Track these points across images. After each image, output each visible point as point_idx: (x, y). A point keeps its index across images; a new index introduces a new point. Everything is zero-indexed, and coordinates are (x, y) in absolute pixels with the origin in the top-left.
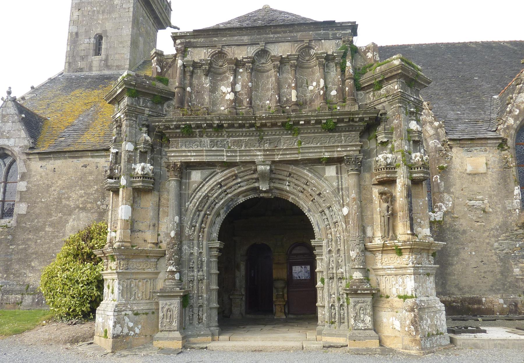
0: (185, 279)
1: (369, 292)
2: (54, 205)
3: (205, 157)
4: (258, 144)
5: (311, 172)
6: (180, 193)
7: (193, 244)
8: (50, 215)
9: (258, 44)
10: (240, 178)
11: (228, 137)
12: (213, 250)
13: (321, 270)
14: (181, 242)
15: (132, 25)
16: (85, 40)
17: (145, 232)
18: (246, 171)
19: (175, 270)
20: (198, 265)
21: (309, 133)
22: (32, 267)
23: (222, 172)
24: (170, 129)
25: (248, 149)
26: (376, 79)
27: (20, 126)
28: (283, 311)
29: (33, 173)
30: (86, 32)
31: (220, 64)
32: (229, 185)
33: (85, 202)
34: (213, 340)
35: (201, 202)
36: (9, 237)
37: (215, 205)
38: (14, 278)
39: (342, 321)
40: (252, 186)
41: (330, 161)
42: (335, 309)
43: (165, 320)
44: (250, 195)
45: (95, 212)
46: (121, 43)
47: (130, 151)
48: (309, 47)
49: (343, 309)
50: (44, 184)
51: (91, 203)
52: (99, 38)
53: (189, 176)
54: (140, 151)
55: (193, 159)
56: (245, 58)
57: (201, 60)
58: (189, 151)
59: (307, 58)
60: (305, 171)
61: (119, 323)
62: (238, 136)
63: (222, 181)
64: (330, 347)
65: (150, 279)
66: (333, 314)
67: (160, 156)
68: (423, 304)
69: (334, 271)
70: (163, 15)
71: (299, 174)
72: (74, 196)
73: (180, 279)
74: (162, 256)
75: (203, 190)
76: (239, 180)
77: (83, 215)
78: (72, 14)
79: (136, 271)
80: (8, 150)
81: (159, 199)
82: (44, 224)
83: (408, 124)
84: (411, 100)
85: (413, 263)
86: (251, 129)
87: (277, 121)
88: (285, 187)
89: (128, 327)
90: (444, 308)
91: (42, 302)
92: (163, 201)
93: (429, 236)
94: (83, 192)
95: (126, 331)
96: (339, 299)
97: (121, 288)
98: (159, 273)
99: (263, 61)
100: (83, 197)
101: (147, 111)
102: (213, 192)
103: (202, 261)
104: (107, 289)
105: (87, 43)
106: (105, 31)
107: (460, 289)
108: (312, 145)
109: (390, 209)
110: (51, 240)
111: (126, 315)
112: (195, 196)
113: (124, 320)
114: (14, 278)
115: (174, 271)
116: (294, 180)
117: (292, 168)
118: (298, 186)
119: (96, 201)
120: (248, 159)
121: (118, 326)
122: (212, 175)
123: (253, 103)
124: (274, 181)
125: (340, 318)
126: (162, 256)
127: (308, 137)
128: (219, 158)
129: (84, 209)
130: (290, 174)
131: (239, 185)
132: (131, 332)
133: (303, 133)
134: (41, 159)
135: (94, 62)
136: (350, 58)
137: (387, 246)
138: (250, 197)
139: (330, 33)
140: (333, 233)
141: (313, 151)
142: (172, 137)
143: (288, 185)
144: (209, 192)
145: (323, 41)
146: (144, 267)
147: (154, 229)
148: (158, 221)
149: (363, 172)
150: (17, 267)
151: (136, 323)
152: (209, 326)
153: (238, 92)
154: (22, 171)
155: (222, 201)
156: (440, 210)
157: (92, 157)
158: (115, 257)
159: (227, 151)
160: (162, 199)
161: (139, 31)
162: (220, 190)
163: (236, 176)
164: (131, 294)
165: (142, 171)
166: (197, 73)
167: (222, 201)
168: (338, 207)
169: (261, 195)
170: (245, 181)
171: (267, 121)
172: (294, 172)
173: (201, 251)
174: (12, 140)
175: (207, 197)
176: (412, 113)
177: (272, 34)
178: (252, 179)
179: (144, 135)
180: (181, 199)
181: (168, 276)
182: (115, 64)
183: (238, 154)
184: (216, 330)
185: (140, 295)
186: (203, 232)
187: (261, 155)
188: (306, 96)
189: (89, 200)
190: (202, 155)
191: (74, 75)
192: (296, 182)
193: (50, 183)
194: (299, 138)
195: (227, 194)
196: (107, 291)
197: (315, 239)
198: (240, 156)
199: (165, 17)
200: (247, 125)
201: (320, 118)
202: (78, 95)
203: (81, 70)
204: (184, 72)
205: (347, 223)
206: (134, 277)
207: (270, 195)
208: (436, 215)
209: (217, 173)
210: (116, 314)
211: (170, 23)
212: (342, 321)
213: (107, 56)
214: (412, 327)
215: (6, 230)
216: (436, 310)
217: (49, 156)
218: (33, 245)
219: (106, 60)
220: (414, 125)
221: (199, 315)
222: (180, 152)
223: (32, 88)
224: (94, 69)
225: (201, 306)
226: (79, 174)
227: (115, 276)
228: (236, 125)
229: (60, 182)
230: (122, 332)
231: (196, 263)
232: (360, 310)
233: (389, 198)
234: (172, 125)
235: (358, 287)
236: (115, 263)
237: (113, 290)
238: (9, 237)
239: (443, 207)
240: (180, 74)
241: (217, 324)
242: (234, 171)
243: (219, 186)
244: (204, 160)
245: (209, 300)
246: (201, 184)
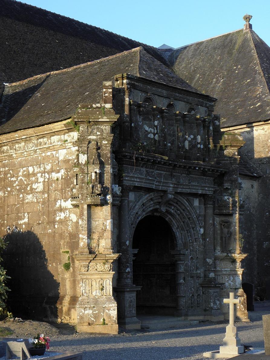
3: (143, 184)
116: (177, 206)
143: (173, 209)
145: (199, 106)
172: (180, 200)
177: (178, 93)
183: (161, 184)
190: (142, 182)
192: (179, 208)
196: (110, 288)
198: (162, 186)
205: (204, 239)
214: (242, 306)
244: (143, 186)
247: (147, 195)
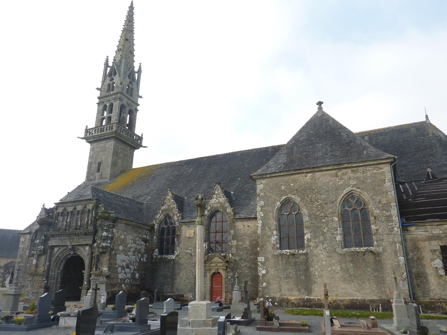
30: (95, 161)
46: (107, 166)
52: (100, 164)
95: (29, 298)
105: (95, 166)
106: (102, 161)
107: (178, 290)
117: (79, 247)
120: (66, 244)
122: (60, 249)
151: (33, 296)
163: (65, 250)
175: (58, 256)
213: (102, 173)
219: (101, 175)
223: (68, 193)
246: (57, 252)
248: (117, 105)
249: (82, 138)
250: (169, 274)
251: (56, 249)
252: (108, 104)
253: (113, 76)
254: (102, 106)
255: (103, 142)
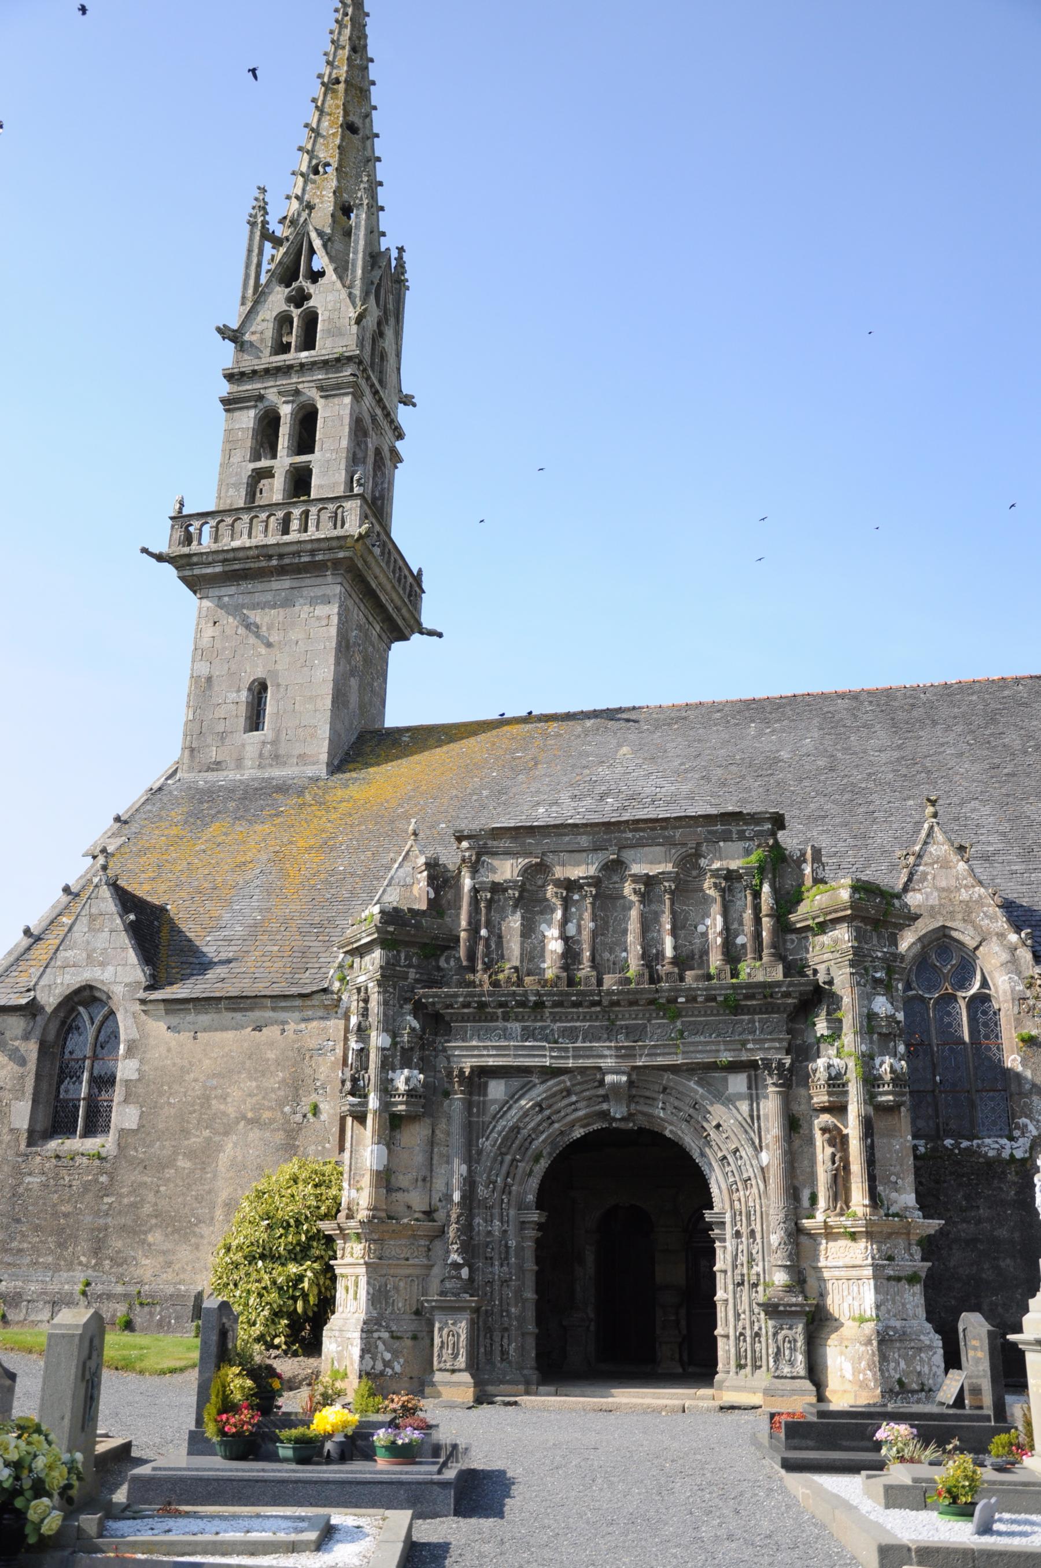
0: (479, 1278)
1: (798, 1309)
2: (195, 1111)
4: (605, 1036)
5: (702, 1087)
6: (470, 1122)
7: (491, 1216)
8: (185, 1132)
9: (607, 849)
10: (576, 1094)
11: (554, 1021)
12: (527, 1226)
13: (724, 1268)
14: (471, 1210)
15: (336, 656)
16: (228, 694)
17: (408, 1191)
18: (586, 1082)
19: (461, 1262)
20: (500, 1253)
21: (697, 1016)
22: (150, 1245)
23: (542, 1083)
24: (453, 1008)
25: (588, 1044)
26: (814, 919)
27: (124, 940)
28: (677, 1356)
29: (152, 1042)
30: (231, 674)
31: (540, 883)
32: (556, 1107)
33: (257, 1108)
34: (527, 1393)
35: (505, 1139)
36: (103, 1179)
37: (530, 1143)
38: (111, 1268)
39: (758, 1364)
40: (597, 1108)
41: (734, 1067)
42: (745, 1341)
43: (444, 1351)
44: (593, 1124)
45: (278, 1130)
47: (383, 1049)
48: (698, 855)
49: (760, 1342)
50: (174, 1065)
51: (270, 1108)
52: (259, 690)
53: (483, 1089)
54: (402, 1047)
55: (491, 1062)
56: (583, 878)
57: (505, 881)
58: (486, 1048)
59: (694, 873)
60: (692, 1084)
61: (369, 1351)
62: (572, 1020)
63: (542, 1099)
64: (733, 1408)
65: (417, 1277)
66: (742, 1350)
67: (434, 1053)
68: (891, 1333)
69: (745, 1271)
70: (404, 611)
71: (681, 1089)
72: (235, 1093)
73: (471, 1279)
74: (437, 1236)
75: (508, 1116)
76: (574, 1098)
77: (254, 1134)
78: (199, 631)
79: (395, 1262)
80: (100, 990)
81: (433, 1131)
82: (175, 1153)
83: (870, 1002)
84: (877, 957)
85: (873, 1258)
86: (593, 1009)
87: (638, 997)
88: (656, 1112)
89: (384, 1360)
90: (940, 1344)
91: (170, 1322)
92: (440, 1135)
93: (913, 1208)
94: (254, 1084)
95: (379, 1366)
96: (752, 1323)
97: (371, 1291)
98: (432, 1266)
99: (616, 878)
100: (255, 1095)
101: (412, 974)
102: (527, 1119)
103: (507, 1247)
104: (344, 1292)
106: (274, 673)
108: (702, 1039)
109: (837, 1158)
110: (189, 1187)
111: (379, 1338)
112: (495, 1127)
113: (377, 1347)
114: (111, 1268)
115: (459, 1264)
116: (672, 1099)
117: (668, 1078)
118: (680, 1110)
119: (281, 1104)
121: (367, 1356)
123: (598, 957)
124: (636, 1100)
125: (754, 1359)
126: (437, 1236)
127: (694, 1023)
128: (537, 1060)
129: (254, 1122)
130: (665, 1089)
131: (573, 1107)
132: (387, 1369)
133: (686, 1016)
134: (168, 1012)
135: (248, 748)
136: (770, 876)
137: (831, 1227)
138: (595, 1127)
139: (734, 829)
140: (743, 1200)
141: (704, 1048)
142: (456, 1021)
144: (520, 1120)
145: (721, 844)
146: (408, 1255)
147: (424, 1187)
148: (431, 1171)
149: (797, 1086)
150: (119, 1244)
151: (396, 1354)
152: (521, 1368)
153: (572, 937)
154: (131, 1037)
155: (544, 1136)
156: (1023, 1135)
157: (274, 1009)
158: (362, 1236)
159: (552, 1049)
160: (437, 1132)
161: (350, 663)
162: (540, 1117)
164: (387, 1303)
165: (406, 1084)
166: (499, 900)
167: (544, 1136)
168: (750, 1151)
169: (614, 1125)
170: (584, 1099)
171: (621, 997)
173: (505, 1227)
174: (110, 969)
175: (516, 1129)
176: (877, 981)
177: (631, 831)
178: (598, 1096)
179: (408, 1018)
180: (473, 1131)
181: (449, 1272)
182: (296, 752)
184: (534, 1376)
185: (400, 1305)
186: (510, 1193)
187: (611, 1056)
188: (691, 944)
189: (266, 1103)
191: (203, 779)
192: (677, 1103)
193: (186, 1063)
194: (678, 1024)
195: (553, 1122)
197: (712, 1208)
199: (407, 615)
200: (586, 1004)
201: (714, 992)
202: (219, 840)
203: (217, 766)
204: (475, 902)
206: (392, 1272)
207: (631, 1125)
208: (1016, 1145)
209: (535, 1086)
210: (364, 1336)
211: (419, 624)
212: (758, 1364)
213: (278, 732)
214: (868, 1372)
215: (97, 1162)
216: (919, 1345)
217: (187, 1006)
218: (151, 1197)
220: (880, 1004)
221: (502, 1346)
222: (469, 1053)
224: (248, 763)
225: (506, 1329)
226: (246, 1045)
227: (362, 1270)
228: (565, 1004)
229: (207, 1062)
230: (373, 1368)
231: (496, 1251)
232: (784, 1342)
233: (838, 1141)
234: (456, 1002)
235: (781, 1299)
236: (361, 1246)
237: (356, 1293)
238: (103, 1179)
239: (1031, 1127)
240: (470, 904)
241: (533, 1363)
242: (564, 1082)
243: (537, 1109)
245: (521, 1319)
247: (550, 1083)
248: (341, 418)
249: (160, 558)
250: (1003, 1233)
251: (497, 1090)
252: (286, 411)
253: (302, 282)
254: (252, 413)
255: (275, 585)
